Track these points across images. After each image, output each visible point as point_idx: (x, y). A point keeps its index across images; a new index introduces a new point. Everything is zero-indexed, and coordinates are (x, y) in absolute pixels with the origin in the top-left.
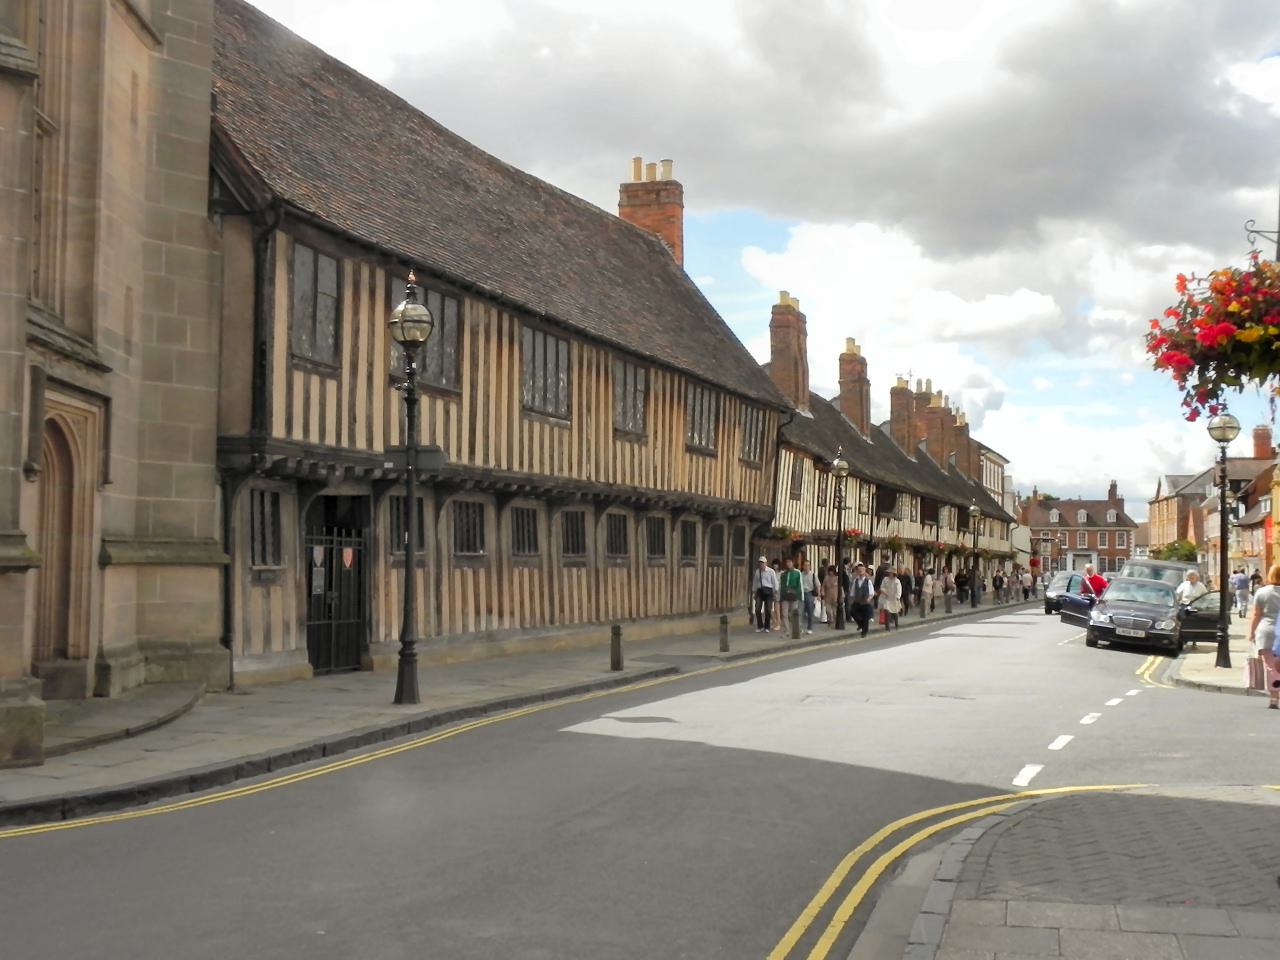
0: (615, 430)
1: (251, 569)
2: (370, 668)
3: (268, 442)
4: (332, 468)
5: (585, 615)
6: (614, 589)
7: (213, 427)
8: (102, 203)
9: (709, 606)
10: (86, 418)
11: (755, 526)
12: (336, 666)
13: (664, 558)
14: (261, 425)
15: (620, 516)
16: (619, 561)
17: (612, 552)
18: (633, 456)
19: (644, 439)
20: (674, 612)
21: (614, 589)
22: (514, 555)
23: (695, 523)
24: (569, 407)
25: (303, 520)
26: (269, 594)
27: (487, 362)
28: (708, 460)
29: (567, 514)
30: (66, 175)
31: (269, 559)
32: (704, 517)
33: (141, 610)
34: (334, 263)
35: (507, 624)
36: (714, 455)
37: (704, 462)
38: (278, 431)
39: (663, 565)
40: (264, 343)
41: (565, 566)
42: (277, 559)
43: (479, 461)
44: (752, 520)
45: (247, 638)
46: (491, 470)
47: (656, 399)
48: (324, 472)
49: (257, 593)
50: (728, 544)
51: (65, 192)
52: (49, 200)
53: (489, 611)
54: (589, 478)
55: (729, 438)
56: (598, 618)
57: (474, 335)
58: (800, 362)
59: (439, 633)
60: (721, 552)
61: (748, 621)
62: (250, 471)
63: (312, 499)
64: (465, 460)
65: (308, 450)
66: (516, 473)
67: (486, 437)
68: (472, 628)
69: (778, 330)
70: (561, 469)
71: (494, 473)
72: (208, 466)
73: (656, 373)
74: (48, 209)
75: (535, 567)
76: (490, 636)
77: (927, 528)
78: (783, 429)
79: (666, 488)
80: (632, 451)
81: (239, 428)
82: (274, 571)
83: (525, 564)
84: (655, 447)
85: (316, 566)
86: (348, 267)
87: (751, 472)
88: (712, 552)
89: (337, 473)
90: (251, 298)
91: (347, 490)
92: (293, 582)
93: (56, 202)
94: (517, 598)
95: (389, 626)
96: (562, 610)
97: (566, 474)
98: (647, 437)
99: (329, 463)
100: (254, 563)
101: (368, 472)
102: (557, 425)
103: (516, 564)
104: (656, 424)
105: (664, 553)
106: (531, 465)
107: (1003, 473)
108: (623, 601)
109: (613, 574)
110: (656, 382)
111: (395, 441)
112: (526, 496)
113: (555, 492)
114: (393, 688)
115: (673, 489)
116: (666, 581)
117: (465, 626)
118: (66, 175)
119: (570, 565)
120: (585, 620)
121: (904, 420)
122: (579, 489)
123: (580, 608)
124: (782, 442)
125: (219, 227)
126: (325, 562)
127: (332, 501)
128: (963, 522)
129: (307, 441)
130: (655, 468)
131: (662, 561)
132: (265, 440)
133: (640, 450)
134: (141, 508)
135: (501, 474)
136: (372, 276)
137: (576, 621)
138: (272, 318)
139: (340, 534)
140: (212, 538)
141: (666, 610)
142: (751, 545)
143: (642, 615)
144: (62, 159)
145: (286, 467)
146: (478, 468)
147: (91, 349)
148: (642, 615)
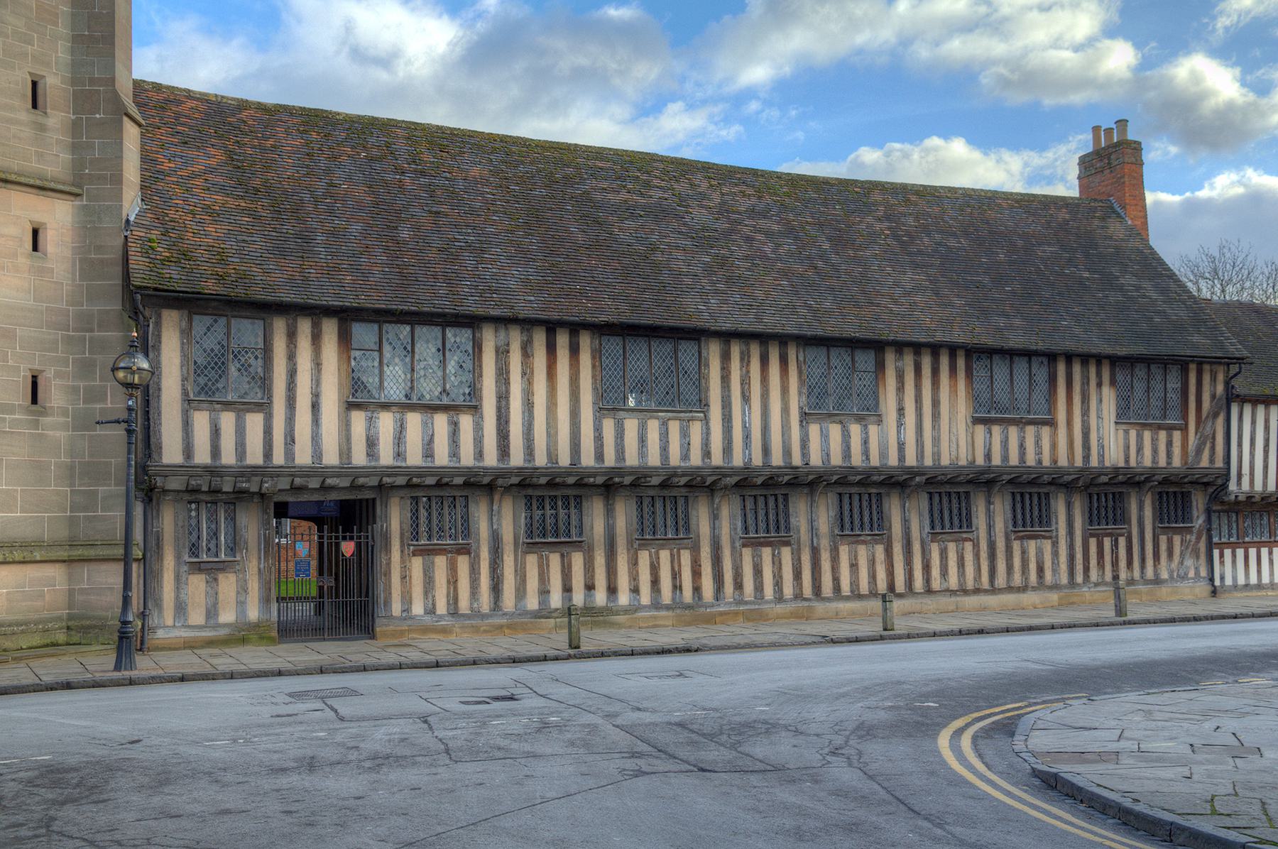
2: (373, 637)
11: (1211, 490)
17: (1161, 521)
33: (71, 593)
35: (624, 598)
41: (744, 545)
78: (1233, 382)
84: (900, 424)
96: (739, 585)
104: (900, 401)
129: (217, 464)
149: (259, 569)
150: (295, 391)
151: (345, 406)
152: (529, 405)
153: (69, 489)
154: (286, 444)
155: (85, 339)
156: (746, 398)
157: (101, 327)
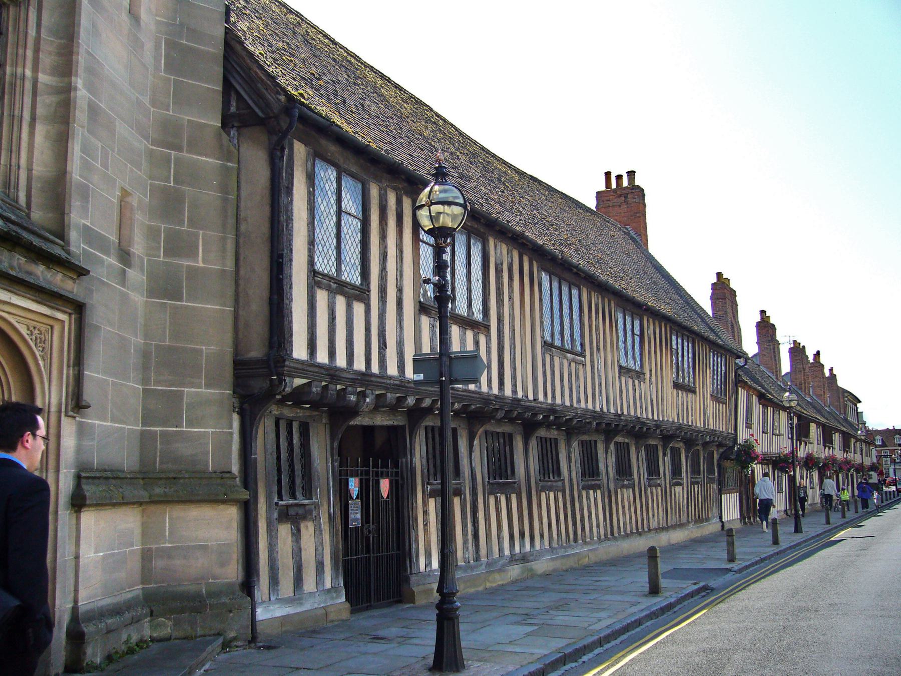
0: (620, 367)
1: (277, 504)
3: (287, 363)
4: (363, 395)
5: (602, 533)
6: (623, 507)
7: (229, 349)
8: (79, 82)
9: (693, 518)
10: (52, 327)
11: (721, 450)
12: (378, 600)
13: (660, 479)
14: (280, 346)
15: (624, 443)
16: (626, 482)
18: (634, 390)
19: (642, 376)
20: (669, 524)
21: (623, 507)
22: (540, 480)
23: (679, 449)
24: (582, 345)
25: (335, 452)
26: (299, 530)
27: (511, 298)
28: (690, 395)
29: (582, 442)
30: (37, 50)
31: (299, 494)
32: (685, 443)
33: (147, 556)
34: (360, 186)
36: (694, 392)
37: (687, 397)
38: (299, 352)
39: (659, 485)
40: (281, 256)
41: (583, 489)
42: (308, 492)
43: (508, 392)
44: (720, 445)
45: (274, 581)
46: (519, 400)
47: (649, 342)
48: (353, 398)
49: (284, 531)
50: (703, 466)
51: (35, 69)
52: (14, 75)
53: (522, 535)
54: (602, 409)
55: (703, 378)
56: (612, 534)
57: (499, 271)
58: (735, 325)
59: (477, 558)
60: (699, 473)
61: (720, 528)
62: (268, 396)
63: (344, 427)
64: (495, 390)
65: (331, 373)
66: (541, 403)
67: (514, 369)
68: (507, 552)
69: (717, 302)
70: (579, 401)
71: (522, 403)
72: (224, 392)
73: (648, 321)
74: (13, 85)
75: (560, 491)
76: (524, 558)
77: (827, 449)
79: (661, 419)
80: (634, 385)
81: (256, 351)
82: (304, 505)
83: (550, 489)
85: (351, 498)
86: (374, 192)
87: (719, 405)
88: (693, 472)
89: (368, 400)
90: (267, 210)
91: (381, 420)
92: (327, 515)
93: (23, 77)
94: (545, 520)
95: (428, 555)
96: (583, 529)
97: (583, 405)
98: (644, 374)
99: (359, 389)
100: (280, 498)
101: (401, 400)
102: (573, 360)
103: (543, 489)
104: (650, 363)
105: (659, 475)
106: (554, 397)
107: (857, 410)
108: (631, 518)
109: (622, 495)
110: (648, 328)
111: (426, 349)
112: (549, 426)
113: (575, 421)
114: (430, 650)
115: (666, 419)
116: (662, 498)
117: (501, 550)
118: (37, 50)
119: (587, 488)
120: (603, 537)
121: (800, 371)
122: (594, 418)
123: (598, 526)
124: (738, 382)
125: (236, 142)
126: (362, 494)
127: (369, 431)
128: (846, 447)
130: (652, 401)
131: (658, 482)
132: (284, 361)
133: (640, 385)
134: (145, 439)
135: (528, 404)
136: (399, 202)
137: (595, 538)
138: (290, 230)
139: (375, 465)
140: (230, 472)
141: (663, 524)
142: (719, 465)
143: (646, 529)
144: (32, 32)
145: (311, 392)
146: (507, 398)
147: (62, 247)
148: (646, 529)
149: (330, 514)
150: (386, 280)
151: (418, 307)
152: (513, 331)
153: (140, 387)
154: (379, 348)
155: (169, 161)
156: (598, 349)
157: (193, 146)
